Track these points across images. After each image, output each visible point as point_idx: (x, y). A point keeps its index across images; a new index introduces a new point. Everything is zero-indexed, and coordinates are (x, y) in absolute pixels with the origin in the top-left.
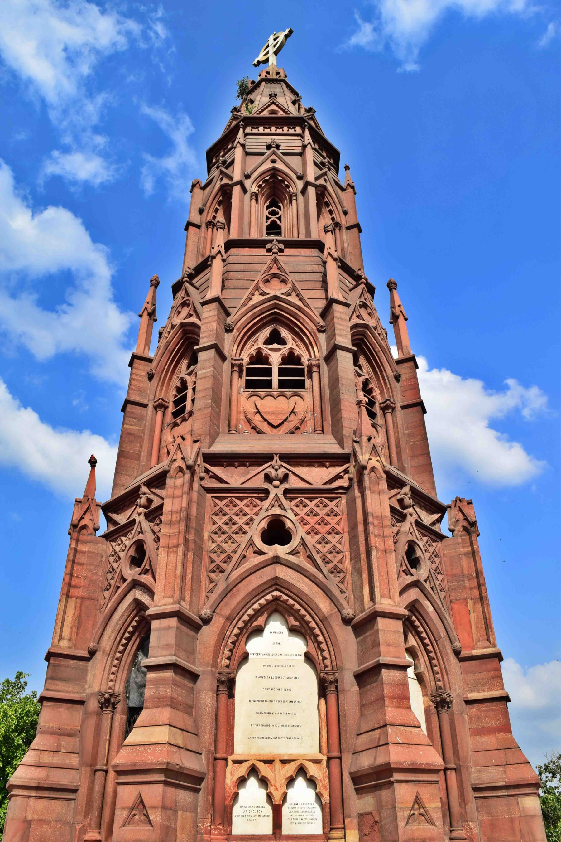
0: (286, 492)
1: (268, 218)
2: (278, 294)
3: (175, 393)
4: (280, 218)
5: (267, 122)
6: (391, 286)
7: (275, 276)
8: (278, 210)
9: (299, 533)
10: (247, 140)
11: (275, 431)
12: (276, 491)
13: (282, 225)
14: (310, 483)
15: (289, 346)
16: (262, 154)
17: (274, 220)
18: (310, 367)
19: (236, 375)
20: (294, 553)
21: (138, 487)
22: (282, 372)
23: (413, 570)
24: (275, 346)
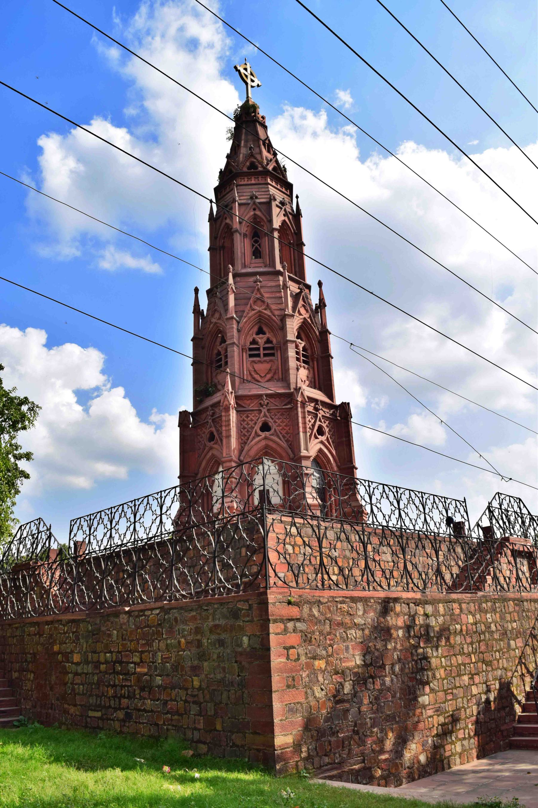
0: (268, 410)
1: (253, 246)
2: (260, 309)
3: (215, 356)
4: (259, 245)
5: (248, 175)
6: (320, 284)
7: (258, 299)
8: (258, 239)
9: (274, 427)
10: (239, 191)
11: (263, 379)
12: (264, 410)
13: (261, 250)
14: (277, 406)
15: (268, 335)
16: (248, 204)
17: (256, 248)
18: (277, 347)
19: (244, 354)
20: (272, 435)
21: (207, 408)
22: (265, 349)
23: (319, 437)
24: (261, 336)
